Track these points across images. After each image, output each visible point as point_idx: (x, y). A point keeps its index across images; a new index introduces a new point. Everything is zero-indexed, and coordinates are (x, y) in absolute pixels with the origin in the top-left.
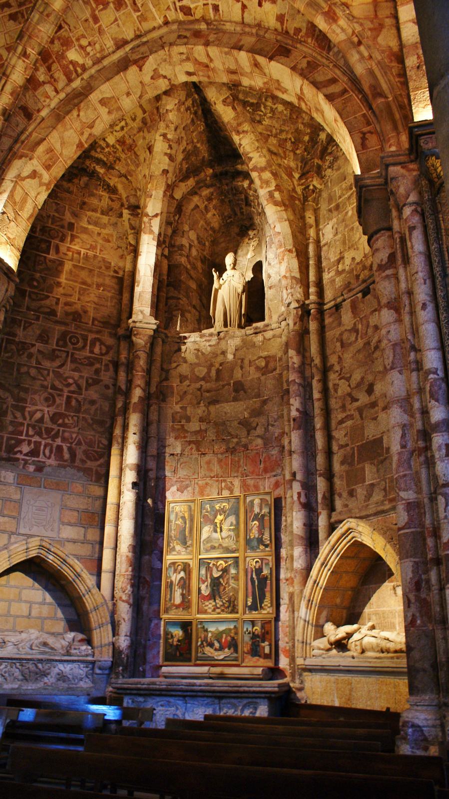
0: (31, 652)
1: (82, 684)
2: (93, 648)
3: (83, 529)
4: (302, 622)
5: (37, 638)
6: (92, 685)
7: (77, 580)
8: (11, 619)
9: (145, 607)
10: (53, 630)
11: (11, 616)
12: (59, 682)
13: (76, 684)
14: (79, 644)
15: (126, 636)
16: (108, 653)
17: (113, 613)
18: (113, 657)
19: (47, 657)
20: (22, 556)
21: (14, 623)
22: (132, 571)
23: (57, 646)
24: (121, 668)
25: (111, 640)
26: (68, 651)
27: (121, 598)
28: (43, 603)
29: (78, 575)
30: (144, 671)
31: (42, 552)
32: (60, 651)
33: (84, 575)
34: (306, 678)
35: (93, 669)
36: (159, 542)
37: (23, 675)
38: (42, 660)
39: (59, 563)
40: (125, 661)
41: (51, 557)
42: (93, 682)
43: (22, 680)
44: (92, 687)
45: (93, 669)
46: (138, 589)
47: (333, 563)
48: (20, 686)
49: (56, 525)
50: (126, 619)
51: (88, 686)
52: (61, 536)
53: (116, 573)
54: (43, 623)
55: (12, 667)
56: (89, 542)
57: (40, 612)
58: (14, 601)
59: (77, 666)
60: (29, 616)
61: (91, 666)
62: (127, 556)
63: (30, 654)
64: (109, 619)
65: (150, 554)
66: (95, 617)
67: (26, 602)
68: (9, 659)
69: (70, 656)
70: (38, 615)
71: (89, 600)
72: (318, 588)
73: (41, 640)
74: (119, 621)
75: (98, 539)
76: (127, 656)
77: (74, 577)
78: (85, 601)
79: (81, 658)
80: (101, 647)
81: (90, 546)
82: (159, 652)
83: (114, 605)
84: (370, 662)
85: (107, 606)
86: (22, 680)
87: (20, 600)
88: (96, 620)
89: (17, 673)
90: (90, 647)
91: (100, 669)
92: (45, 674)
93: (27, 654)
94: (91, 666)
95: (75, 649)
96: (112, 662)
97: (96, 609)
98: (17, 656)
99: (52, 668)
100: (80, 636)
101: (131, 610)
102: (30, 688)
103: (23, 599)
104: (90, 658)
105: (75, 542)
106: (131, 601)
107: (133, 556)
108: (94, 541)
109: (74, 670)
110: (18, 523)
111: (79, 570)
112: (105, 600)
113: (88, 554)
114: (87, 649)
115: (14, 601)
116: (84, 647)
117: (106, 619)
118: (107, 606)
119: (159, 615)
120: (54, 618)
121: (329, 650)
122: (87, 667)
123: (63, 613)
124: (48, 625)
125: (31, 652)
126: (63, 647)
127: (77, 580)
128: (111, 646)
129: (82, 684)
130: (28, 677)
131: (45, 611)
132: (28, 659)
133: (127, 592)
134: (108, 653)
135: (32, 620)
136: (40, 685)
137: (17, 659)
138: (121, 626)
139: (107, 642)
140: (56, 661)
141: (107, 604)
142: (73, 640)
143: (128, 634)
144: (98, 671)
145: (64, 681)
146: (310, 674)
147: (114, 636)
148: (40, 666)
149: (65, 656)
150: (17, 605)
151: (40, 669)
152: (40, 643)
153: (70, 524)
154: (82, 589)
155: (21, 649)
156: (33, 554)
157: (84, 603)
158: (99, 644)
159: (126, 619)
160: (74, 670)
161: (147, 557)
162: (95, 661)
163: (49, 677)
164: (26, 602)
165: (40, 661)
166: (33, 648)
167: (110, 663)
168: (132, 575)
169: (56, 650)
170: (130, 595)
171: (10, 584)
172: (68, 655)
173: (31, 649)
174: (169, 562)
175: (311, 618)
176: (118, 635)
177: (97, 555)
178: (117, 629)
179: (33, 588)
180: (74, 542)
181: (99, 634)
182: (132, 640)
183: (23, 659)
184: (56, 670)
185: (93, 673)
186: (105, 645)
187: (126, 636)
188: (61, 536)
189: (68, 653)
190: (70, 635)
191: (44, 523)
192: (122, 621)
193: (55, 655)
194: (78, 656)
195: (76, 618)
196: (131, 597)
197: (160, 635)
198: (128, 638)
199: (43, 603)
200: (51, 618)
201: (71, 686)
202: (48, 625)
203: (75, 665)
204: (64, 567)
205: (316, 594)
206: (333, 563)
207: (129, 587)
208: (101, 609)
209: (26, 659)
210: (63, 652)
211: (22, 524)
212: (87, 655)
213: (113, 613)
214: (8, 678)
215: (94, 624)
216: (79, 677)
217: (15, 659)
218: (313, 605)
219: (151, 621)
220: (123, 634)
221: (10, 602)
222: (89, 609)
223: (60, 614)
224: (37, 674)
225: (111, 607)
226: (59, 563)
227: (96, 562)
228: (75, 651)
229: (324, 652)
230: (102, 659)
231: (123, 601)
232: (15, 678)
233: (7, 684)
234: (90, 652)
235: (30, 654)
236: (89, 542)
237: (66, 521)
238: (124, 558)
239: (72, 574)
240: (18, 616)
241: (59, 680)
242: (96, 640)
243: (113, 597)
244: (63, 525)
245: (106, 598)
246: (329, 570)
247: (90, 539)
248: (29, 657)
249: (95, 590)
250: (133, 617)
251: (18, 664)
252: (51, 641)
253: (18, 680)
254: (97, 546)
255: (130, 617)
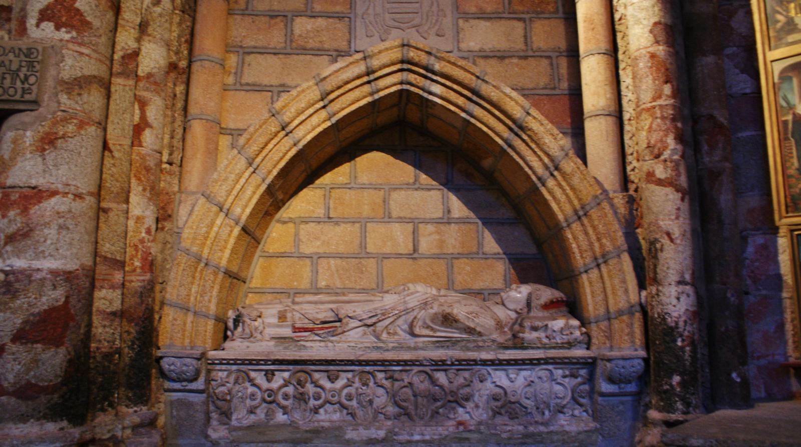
0: (412, 341)
1: (563, 421)
2: (583, 324)
3: (519, 25)
5: (425, 305)
6: (592, 425)
7: (518, 143)
8: (371, 264)
9: (725, 199)
10: (478, 285)
11: (369, 256)
12: (499, 420)
13: (546, 424)
14: (546, 314)
15: (680, 283)
16: (631, 334)
17: (631, 224)
18: (647, 346)
19: (456, 353)
20: (357, 93)
21: (380, 276)
22: (675, 94)
23: (484, 322)
24: (676, 379)
25: (633, 297)
26: (515, 336)
27: (650, 176)
28: (446, 220)
29: (519, 128)
30: (745, 383)
31: (412, 77)
32: (495, 336)
33: (534, 125)
35: (591, 379)
36: (736, 23)
37: (396, 404)
38: (443, 362)
39: (461, 101)
40: (687, 356)
41: (437, 89)
42: (595, 417)
43: (397, 417)
44: (596, 430)
45: (591, 379)
46: (697, 149)
48: (390, 432)
49: (448, 22)
50: (676, 233)
51: (582, 427)
52: (463, 46)
53: (626, 116)
54: (450, 269)
55: (365, 384)
56: (539, 55)
57: (441, 243)
58: (370, 220)
59: (543, 374)
60: (414, 254)
61: (583, 372)
62: (653, 56)
63: (409, 348)
64: (621, 239)
65: (718, 51)
66: (581, 237)
67: (402, 220)
68: (352, 363)
69: (526, 348)
70: (436, 251)
71: (558, 192)
73: (436, 309)
74: (652, 243)
75: (563, 45)
76: (693, 344)
77: (506, 134)
78: (548, 196)
79: (552, 353)
80: (609, 319)
81: (545, 62)
82: (781, 326)
83: (631, 201)
85: (612, 206)
86: (397, 417)
87: (388, 218)
88: (584, 244)
89: (381, 399)
90: (575, 323)
91: (611, 380)
92: (456, 399)
93: (400, 347)
94: (583, 372)
95: (535, 329)
96: (646, 360)
97: (582, 213)
98: (375, 355)
99: (477, 384)
100: (547, 294)
101: (685, 206)
102: (417, 437)
103: (395, 214)
104: (579, 352)
105: (502, 58)
106: (683, 181)
107: (670, 54)
108: (554, 50)
109: (539, 385)
110: (351, 30)
111: (518, 113)
112: (605, 191)
113: (542, 84)
114: (567, 326)
115: (370, 220)
116: (559, 324)
117: (613, 240)
118: (612, 206)
119: (772, 220)
120: (477, 254)
122: (573, 376)
123: (499, 241)
124: (464, 272)
125: (412, 341)
126: (499, 325)
127: (518, 143)
128: (638, 315)
129: (563, 421)
130: (411, 408)
131: (453, 238)
132: (406, 363)
133: (666, 154)
134: (631, 334)
135: (422, 262)
136: (447, 428)
137: (374, 363)
138: (662, 256)
139: (623, 304)
140: (484, 363)
141: (610, 200)
142: (529, 304)
143: (688, 277)
144: (605, 387)
145: (513, 416)
147: (642, 286)
148: (441, 377)
149: (507, 348)
150: (381, 229)
151: (441, 387)
152: (434, 318)
153: (482, 16)
154: (536, 164)
155: (384, 336)
156: (389, 85)
157: (546, 203)
158: (602, 311)
159: (676, 233)
160: (539, 385)
161: (710, 59)
162: (595, 359)
163: (470, 405)
164: (402, 220)
165: (440, 365)
166: (417, 331)
167: (639, 365)
168: (674, 107)
169: (480, 334)
170: (677, 164)
171: (360, 181)
172: (515, 347)
173: (413, 335)
174: (778, 67)
176: (656, 281)
177: (565, 85)
178: (649, 264)
179: (415, 186)
180: (501, 56)
181: (598, 286)
182: (697, 293)
183: (391, 363)
184: (488, 387)
185: (592, 392)
186: (620, 313)
187: (680, 283)
188: (463, 46)
189: (517, 343)
190: (520, 293)
191: (417, 21)
192: (665, 241)
193: (479, 348)
194: (545, 347)
195: (532, 250)
196: (682, 169)
197: (779, 277)
198: (688, 289)
199: (446, 220)
200: (469, 256)
201: (531, 429)
202: (464, 272)
203: (540, 372)
204: (478, 111)
207: (671, 141)
208: (594, 213)
209: (398, 363)
210: (501, 339)
211: (360, 31)
212: (570, 345)
213: (631, 224)
214: (360, 413)
215: (579, 260)
216: (553, 403)
217: (367, 363)
219: (744, 239)
220: (673, 277)
221: (363, 222)
222: (561, 217)
223: (491, 245)
224: (435, 400)
225: (622, 210)
226: (461, 101)
227: (566, 101)
228: (535, 335)
230: (615, 354)
231: (660, 182)
232: (377, 412)
233: (355, 427)
234: (577, 333)
235: (409, 348)
236: (539, 55)
237: (473, 9)
238: (643, 64)
239: (500, 128)
240: (386, 257)
241: (496, 413)
242: (592, 304)
243: (625, 181)
244: (467, 20)
245: (607, 186)
247: (542, 45)
248: (407, 356)
249: (570, 165)
250: (694, 232)
251: (380, 376)
252: (462, 310)
253: (388, 418)
254: (563, 63)
255: (687, 228)
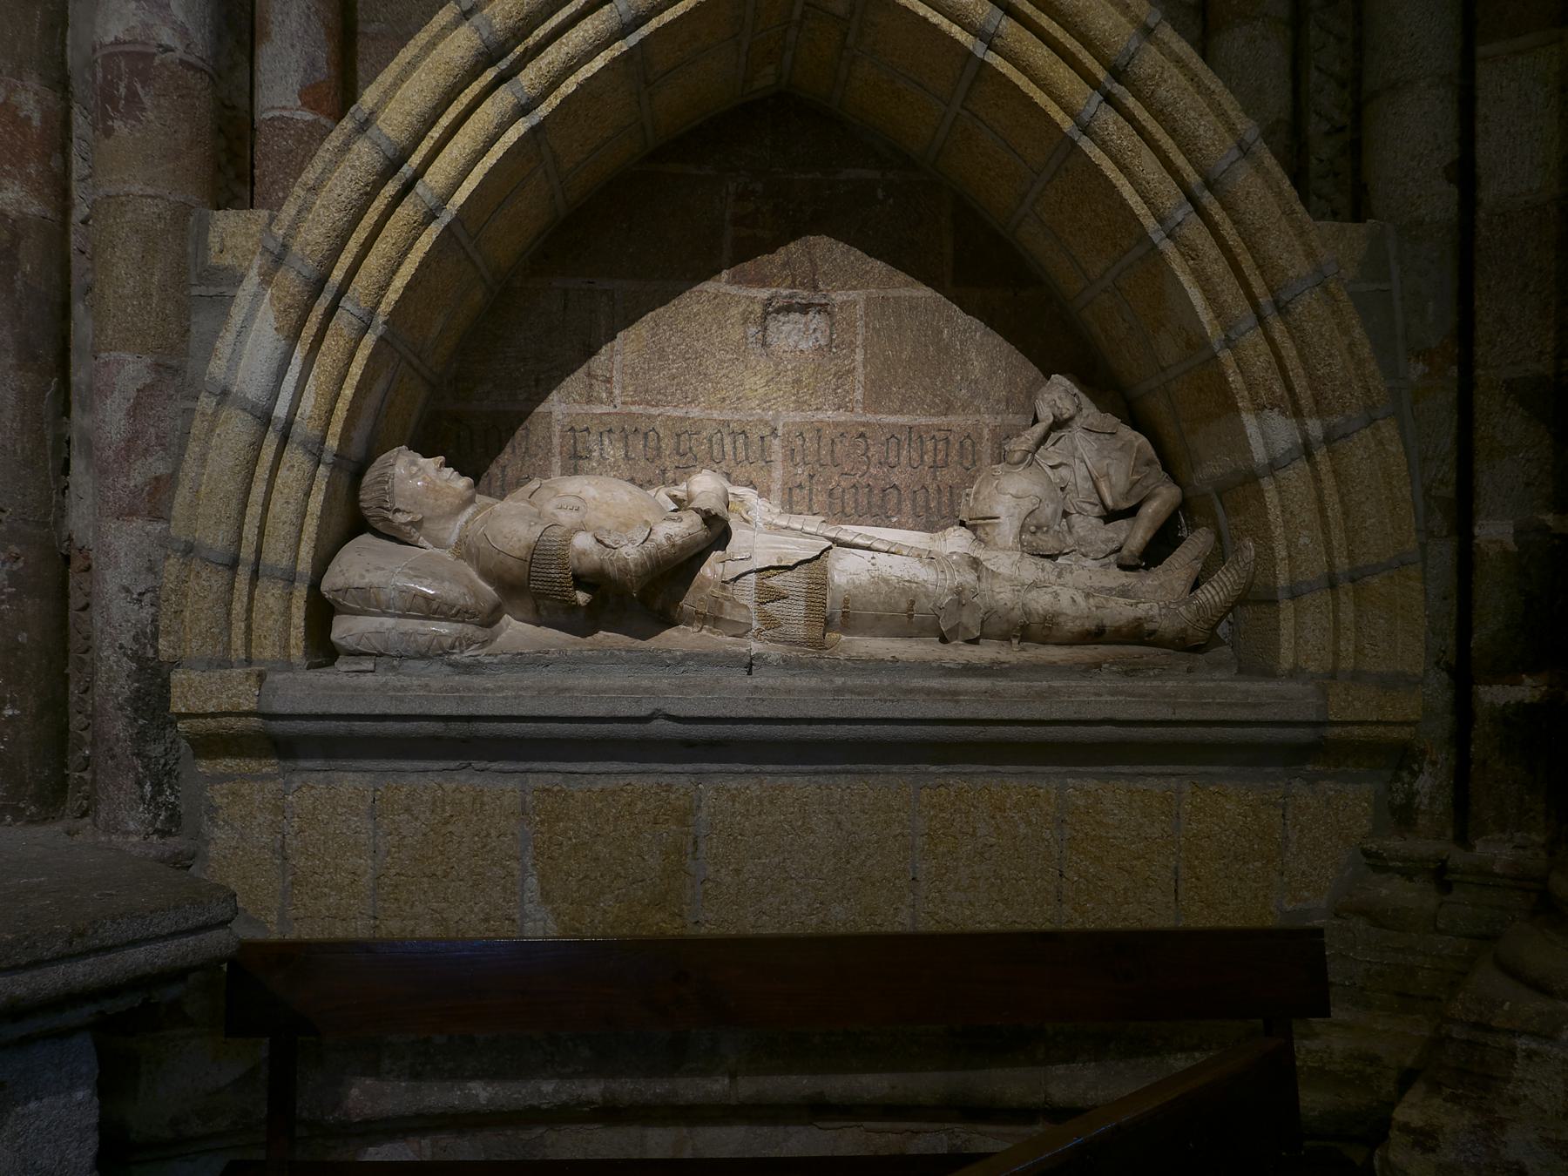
4: (235, 429)
34: (218, 794)
47: (569, 69)
72: (406, 211)
84: (953, 695)
121: (490, 619)
146: (269, 766)
175: (308, 404)
205: (384, 247)
206: (569, 69)
218: (344, 321)
229: (469, 630)
246: (524, 110)
